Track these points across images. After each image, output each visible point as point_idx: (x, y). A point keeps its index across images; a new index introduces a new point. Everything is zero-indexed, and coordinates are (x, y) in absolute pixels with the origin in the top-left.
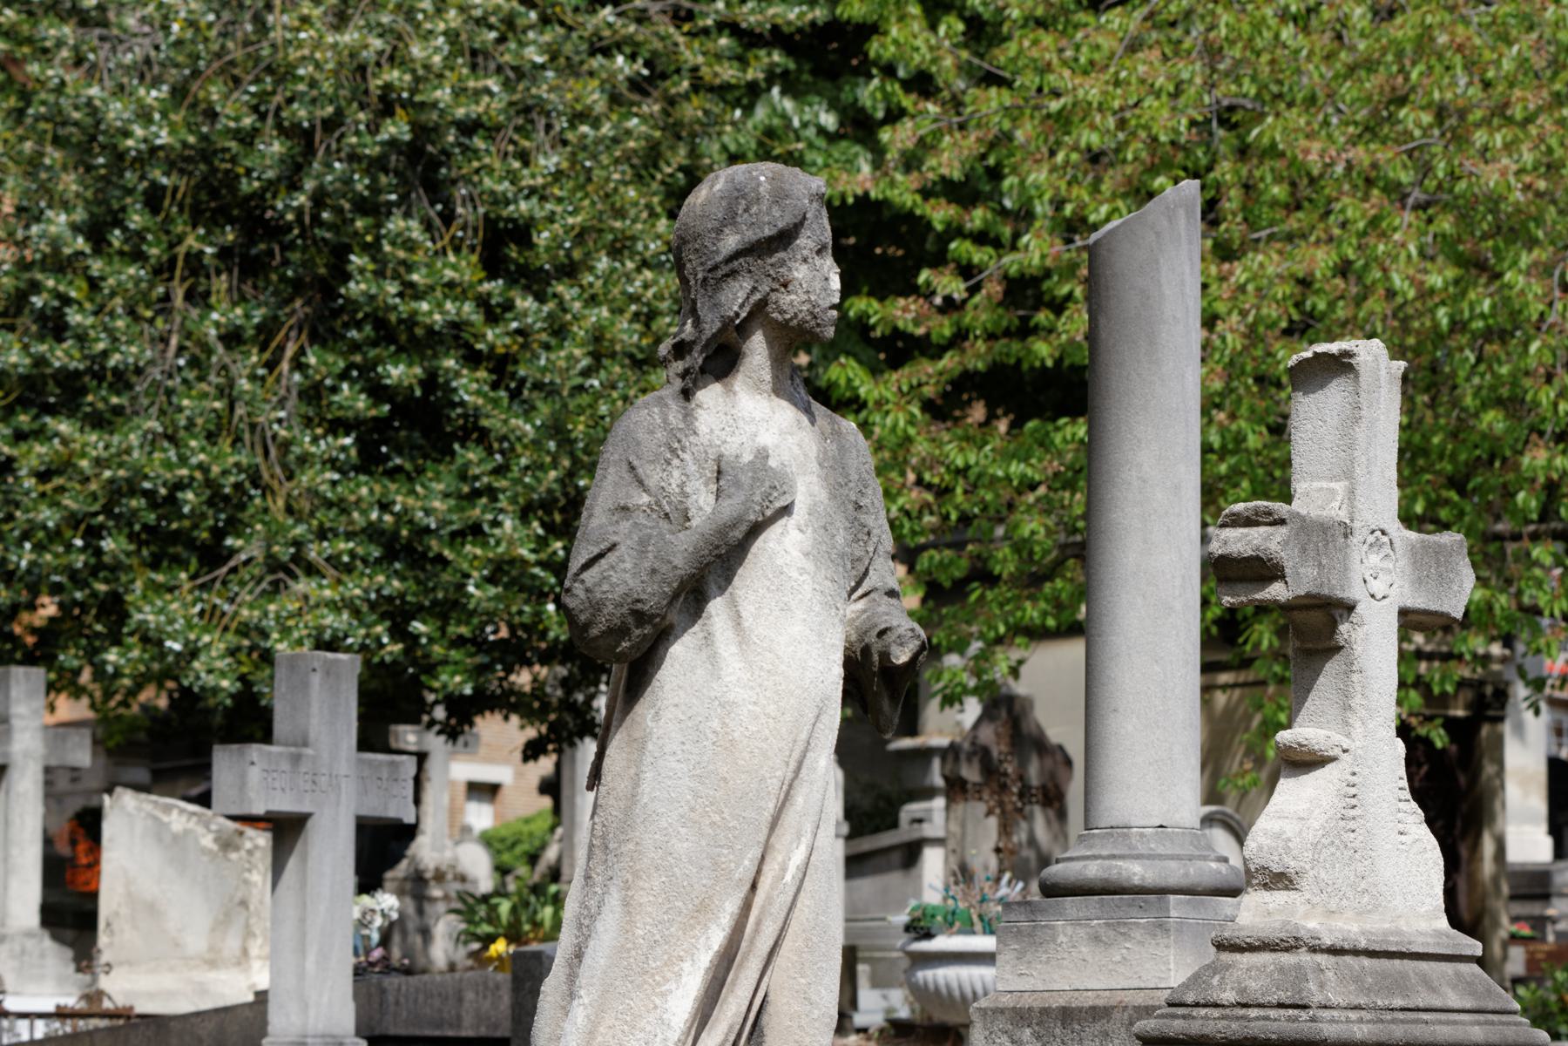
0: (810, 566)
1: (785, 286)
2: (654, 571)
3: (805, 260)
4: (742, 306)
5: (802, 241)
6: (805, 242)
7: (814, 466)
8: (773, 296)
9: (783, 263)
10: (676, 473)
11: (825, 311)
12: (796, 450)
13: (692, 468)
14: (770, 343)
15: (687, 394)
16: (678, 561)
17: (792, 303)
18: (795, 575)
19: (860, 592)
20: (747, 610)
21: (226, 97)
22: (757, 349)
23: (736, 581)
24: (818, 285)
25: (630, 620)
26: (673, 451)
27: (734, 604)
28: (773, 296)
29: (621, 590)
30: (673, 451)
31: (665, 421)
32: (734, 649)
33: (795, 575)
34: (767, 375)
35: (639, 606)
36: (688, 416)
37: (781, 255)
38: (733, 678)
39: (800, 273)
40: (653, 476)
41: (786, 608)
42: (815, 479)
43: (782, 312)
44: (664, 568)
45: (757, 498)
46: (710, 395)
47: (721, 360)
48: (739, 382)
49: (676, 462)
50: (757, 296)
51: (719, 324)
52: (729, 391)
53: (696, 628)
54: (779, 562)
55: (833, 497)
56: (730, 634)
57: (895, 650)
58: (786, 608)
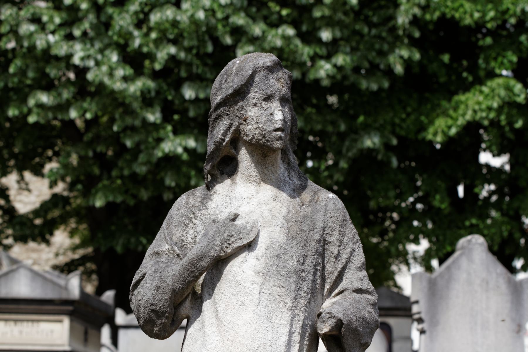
0: (260, 279)
1: (245, 120)
2: (158, 288)
3: (255, 105)
4: (225, 134)
5: (252, 95)
6: (254, 95)
7: (280, 220)
8: (242, 127)
9: (242, 108)
10: (191, 232)
11: (270, 132)
12: (266, 213)
13: (200, 228)
14: (251, 153)
15: (209, 187)
16: (169, 281)
17: (250, 130)
18: (248, 285)
19: (336, 291)
20: (221, 306)
21: (401, 57)
22: (244, 157)
23: (216, 290)
24: (263, 119)
25: (152, 315)
26: (190, 219)
27: (215, 304)
28: (242, 127)
29: (145, 299)
30: (190, 219)
31: (187, 203)
32: (214, 329)
33: (248, 285)
34: (253, 171)
35: (154, 307)
36: (206, 199)
37: (241, 103)
38: (213, 346)
39: (252, 113)
40: (178, 234)
41: (242, 305)
42: (278, 229)
43: (248, 136)
44: (163, 286)
45: (218, 242)
46: (222, 188)
47: (227, 167)
48: (239, 177)
49: (191, 225)
50: (233, 128)
51: (213, 146)
52: (234, 183)
53: (200, 318)
54: (239, 278)
55: (291, 238)
56: (214, 320)
57: (319, 325)
58: (242, 305)
